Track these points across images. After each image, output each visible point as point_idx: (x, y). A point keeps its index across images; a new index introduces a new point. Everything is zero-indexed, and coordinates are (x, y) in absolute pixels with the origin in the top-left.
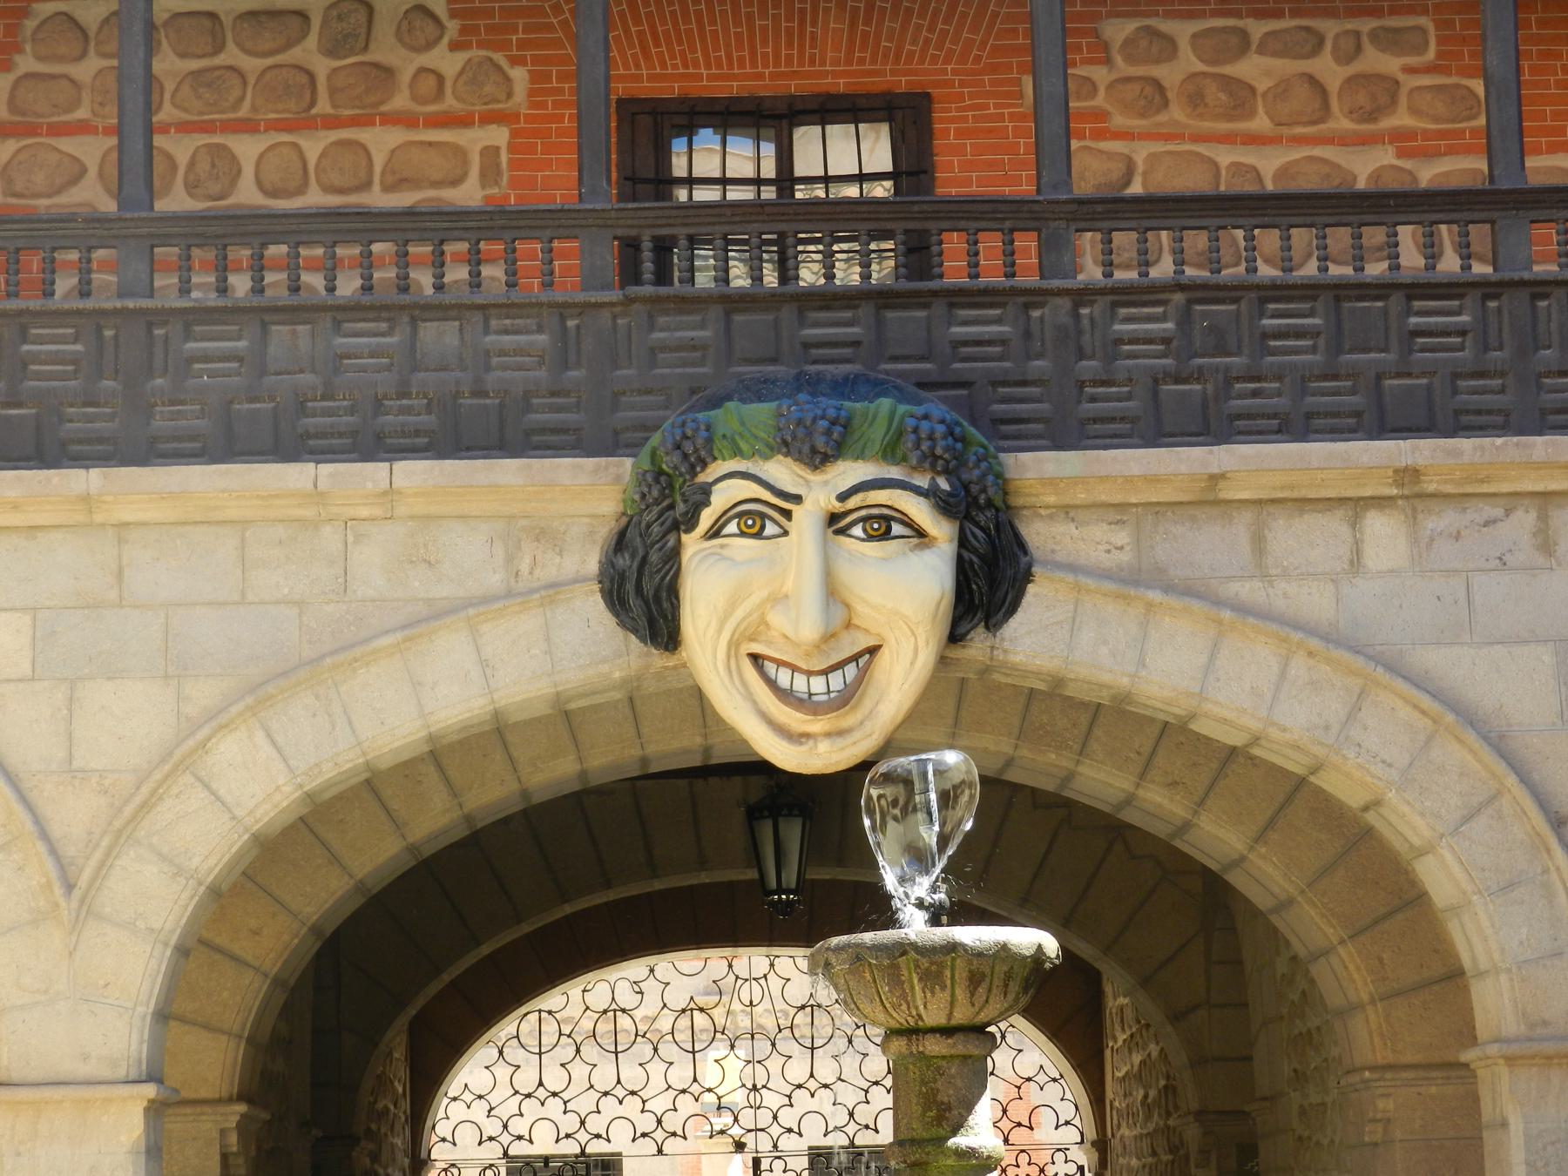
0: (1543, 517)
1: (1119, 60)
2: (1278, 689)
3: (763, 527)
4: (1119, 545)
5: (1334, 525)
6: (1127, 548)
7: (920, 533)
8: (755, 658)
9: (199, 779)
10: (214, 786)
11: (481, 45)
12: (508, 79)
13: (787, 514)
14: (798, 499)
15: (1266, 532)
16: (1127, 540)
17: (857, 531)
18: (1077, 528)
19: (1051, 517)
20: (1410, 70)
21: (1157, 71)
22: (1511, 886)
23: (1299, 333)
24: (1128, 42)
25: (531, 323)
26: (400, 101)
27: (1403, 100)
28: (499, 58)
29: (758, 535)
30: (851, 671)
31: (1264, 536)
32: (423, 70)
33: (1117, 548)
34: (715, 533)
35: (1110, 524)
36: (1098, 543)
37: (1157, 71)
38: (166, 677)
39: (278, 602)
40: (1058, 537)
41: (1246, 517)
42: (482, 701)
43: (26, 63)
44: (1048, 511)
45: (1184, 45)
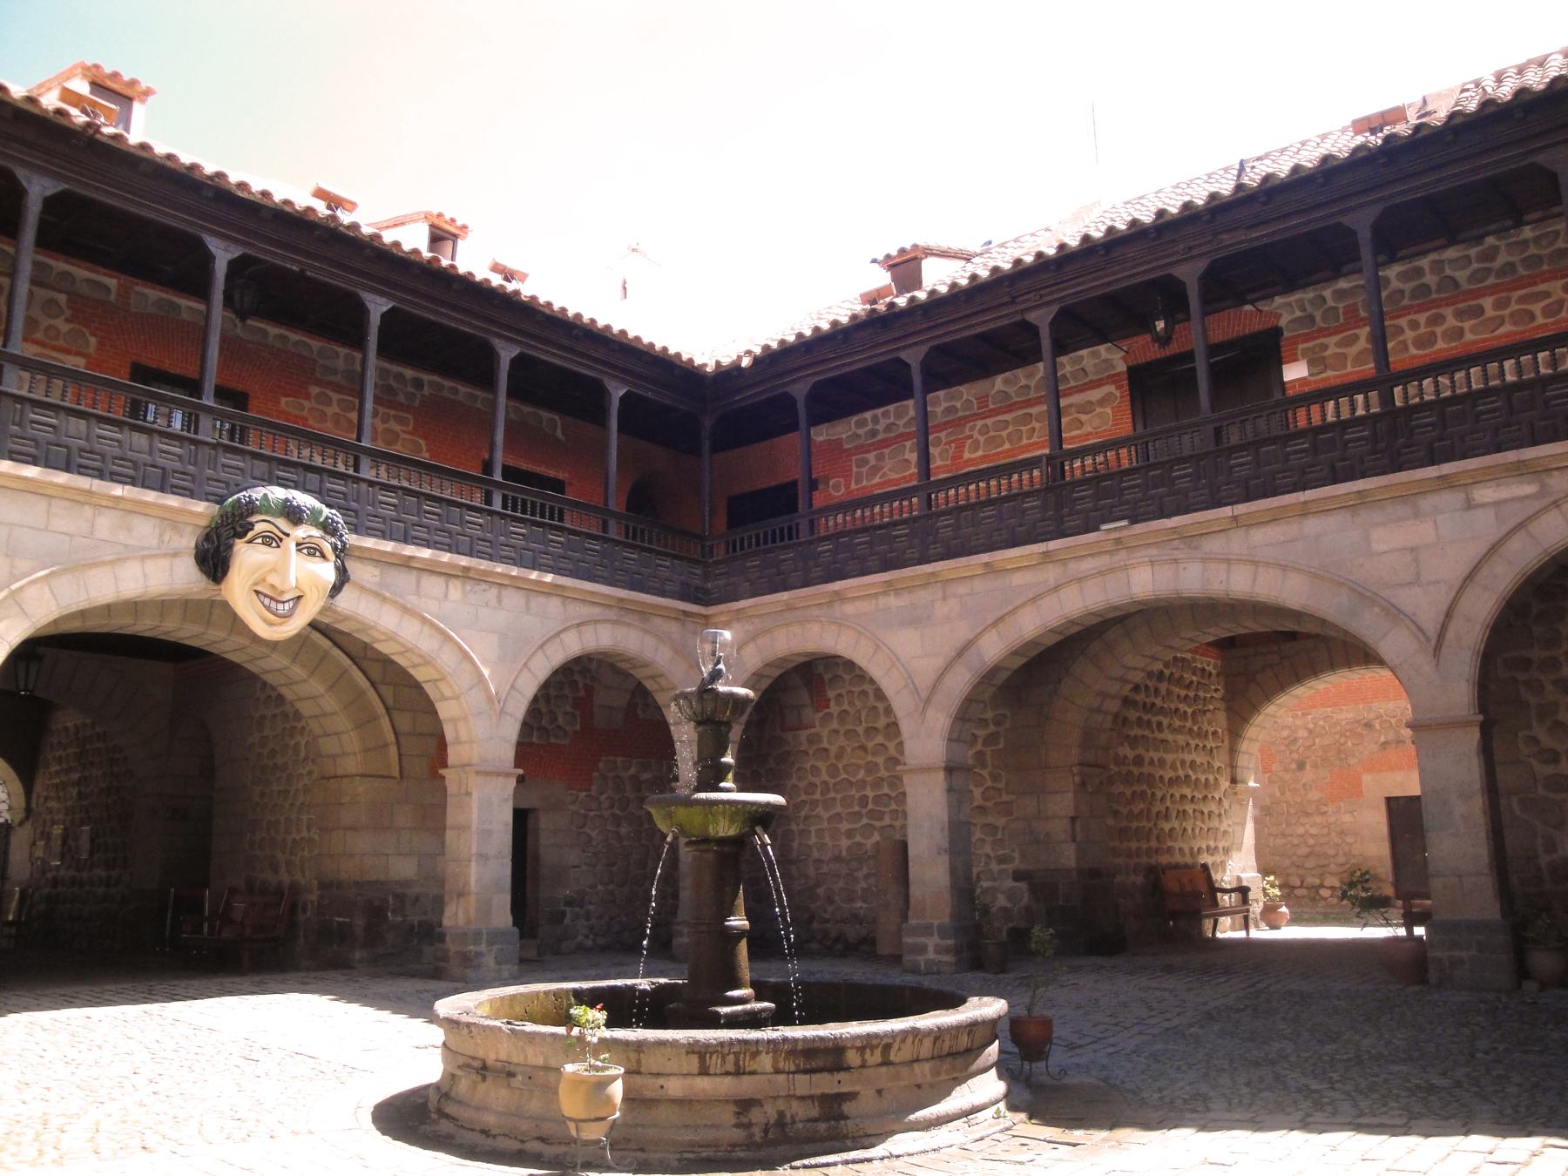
0: (499, 592)
1: (313, 401)
5: (441, 581)
7: (323, 556)
8: (257, 592)
9: (16, 602)
10: (24, 606)
13: (281, 540)
14: (288, 535)
20: (404, 432)
21: (324, 408)
22: (480, 714)
23: (434, 514)
24: (318, 395)
25: (177, 443)
26: (39, 335)
27: (400, 442)
28: (86, 332)
29: (269, 545)
30: (291, 603)
34: (250, 542)
37: (324, 408)
38: (7, 555)
39: (61, 533)
41: (415, 573)
42: (141, 590)
45: (335, 403)
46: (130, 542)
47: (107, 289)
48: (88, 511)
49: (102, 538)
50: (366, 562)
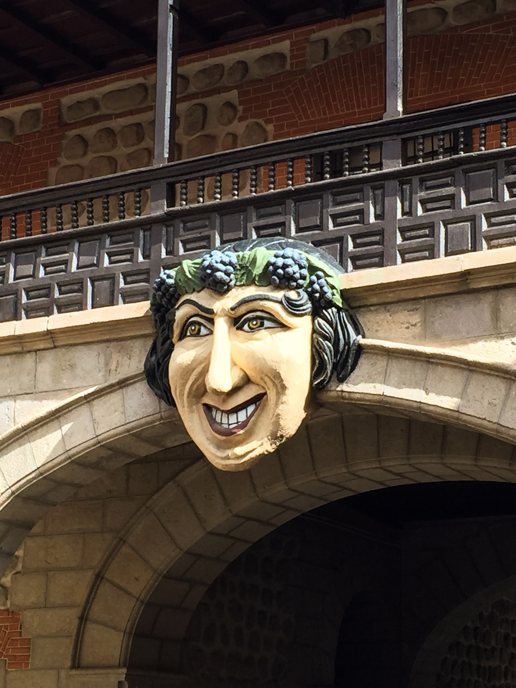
2: (504, 404)
3: (199, 330)
4: (414, 323)
6: (419, 325)
11: (252, 117)
12: (265, 131)
15: (501, 306)
16: (418, 320)
17: (246, 327)
18: (390, 316)
19: (376, 310)
28: (261, 121)
30: (251, 409)
31: (500, 309)
32: (229, 134)
33: (412, 325)
34: (182, 336)
35: (409, 311)
36: (402, 323)
40: (380, 322)
43: (64, 161)
44: (376, 307)
46: (75, 384)
47: (281, 56)
48: (29, 360)
49: (45, 389)
50: (393, 307)
